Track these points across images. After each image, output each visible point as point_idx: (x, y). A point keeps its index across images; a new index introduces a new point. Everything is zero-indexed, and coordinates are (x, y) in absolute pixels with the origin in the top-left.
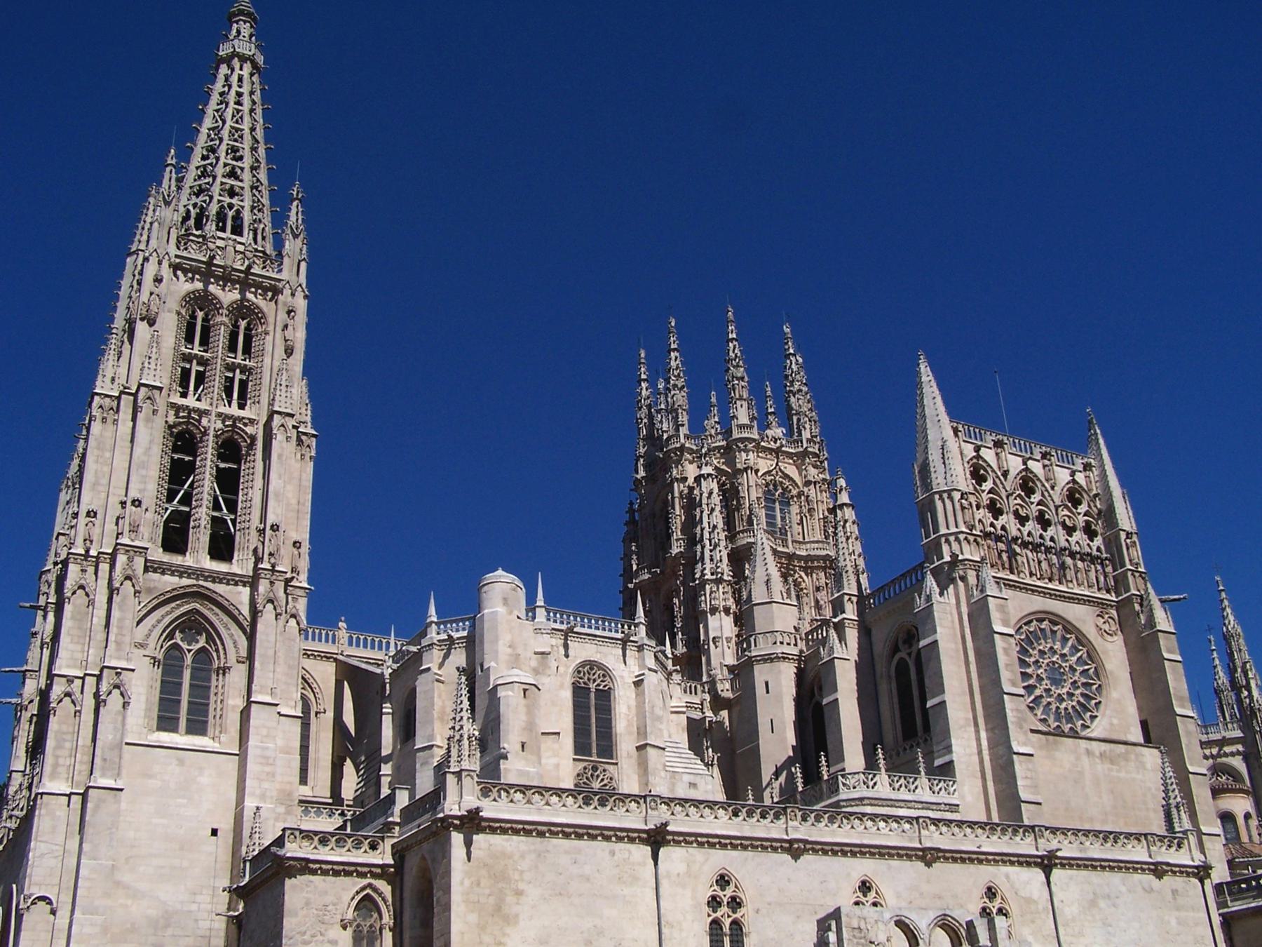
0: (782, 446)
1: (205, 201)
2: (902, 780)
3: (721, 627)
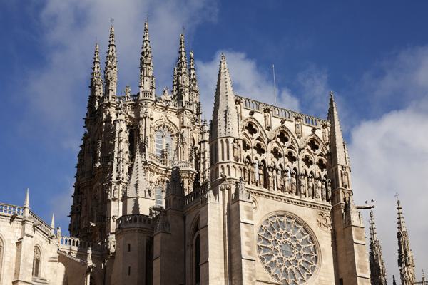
0: (169, 105)
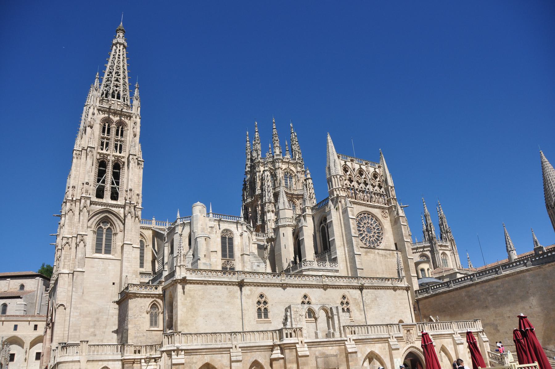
0: (290, 161)
1: (108, 89)
2: (321, 263)
3: (271, 216)
